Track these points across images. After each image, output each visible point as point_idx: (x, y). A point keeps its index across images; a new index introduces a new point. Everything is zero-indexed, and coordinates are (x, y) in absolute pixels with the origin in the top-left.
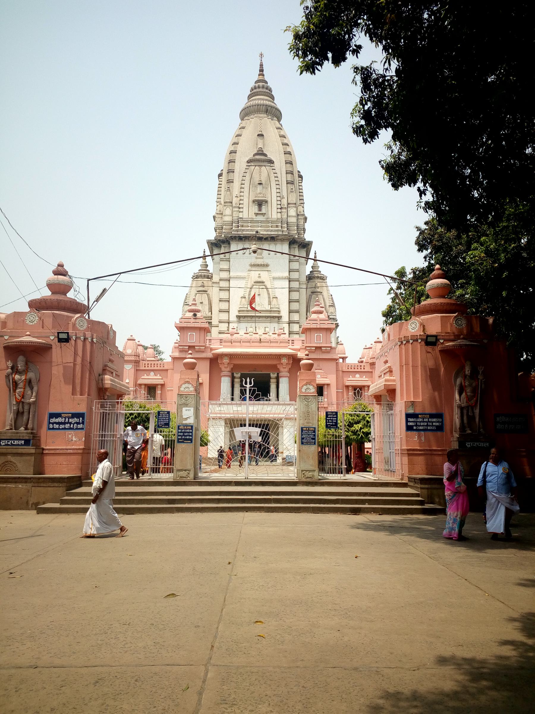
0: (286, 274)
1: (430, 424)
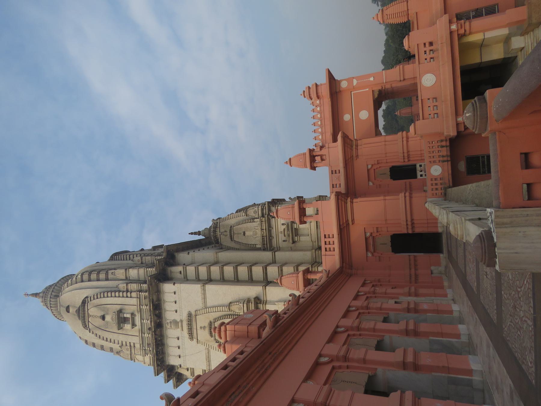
0: (197, 287)
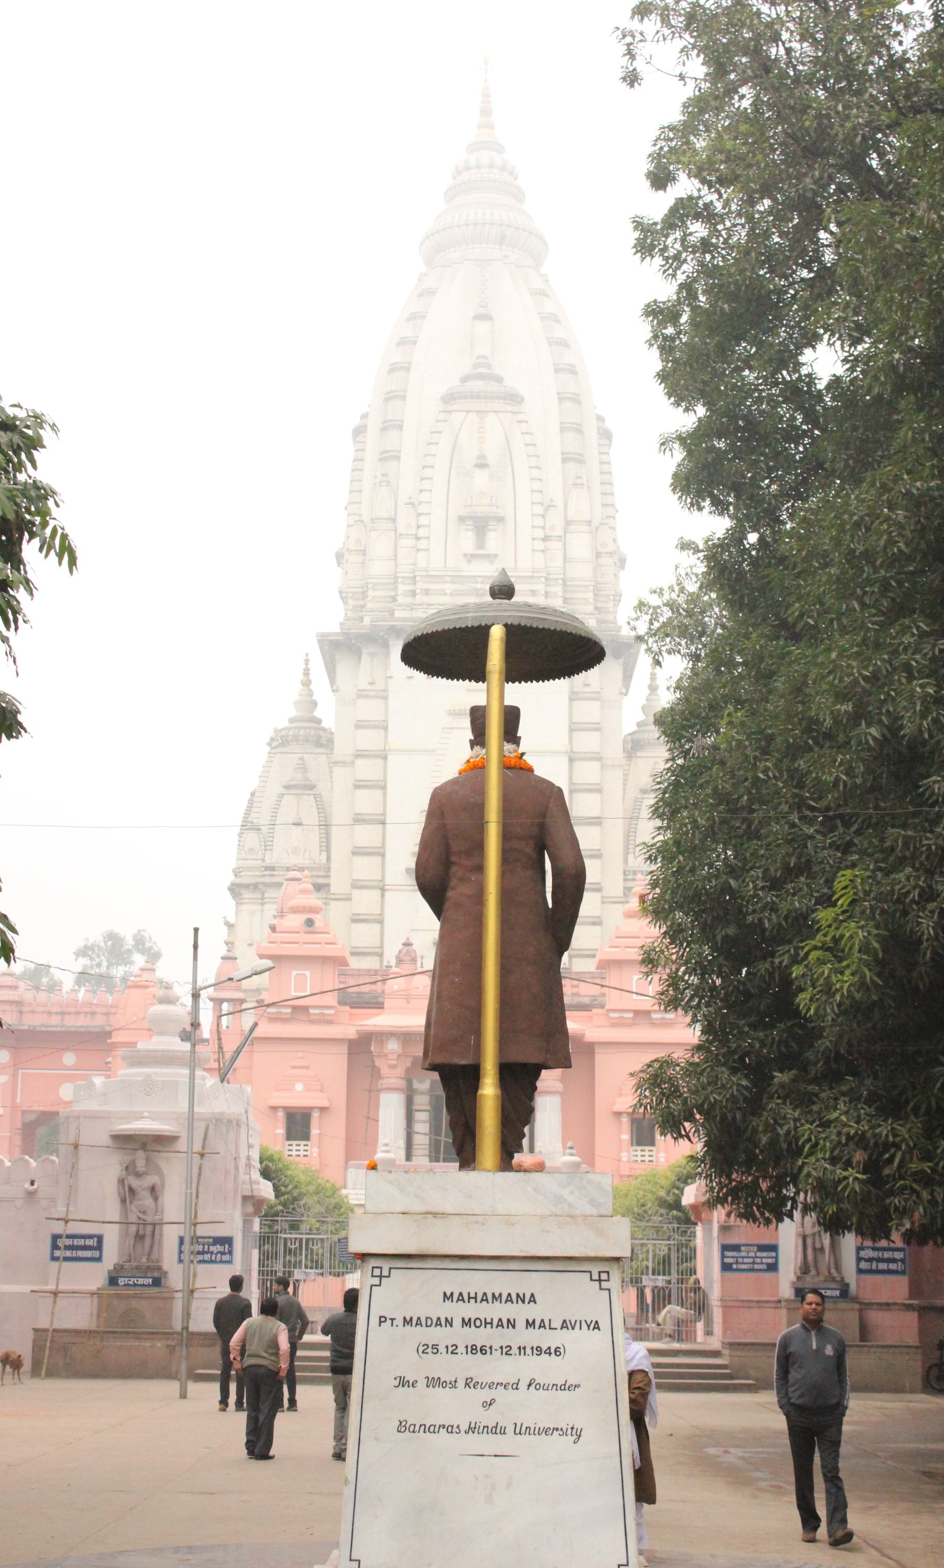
1: (758, 1260)
